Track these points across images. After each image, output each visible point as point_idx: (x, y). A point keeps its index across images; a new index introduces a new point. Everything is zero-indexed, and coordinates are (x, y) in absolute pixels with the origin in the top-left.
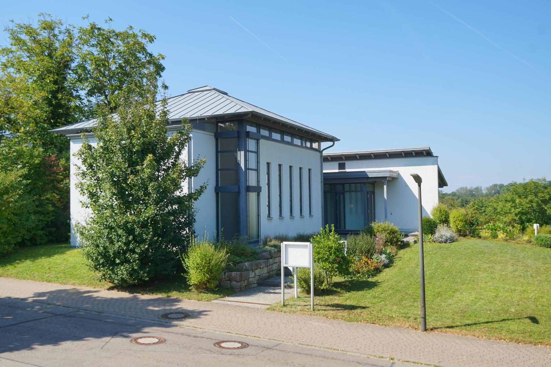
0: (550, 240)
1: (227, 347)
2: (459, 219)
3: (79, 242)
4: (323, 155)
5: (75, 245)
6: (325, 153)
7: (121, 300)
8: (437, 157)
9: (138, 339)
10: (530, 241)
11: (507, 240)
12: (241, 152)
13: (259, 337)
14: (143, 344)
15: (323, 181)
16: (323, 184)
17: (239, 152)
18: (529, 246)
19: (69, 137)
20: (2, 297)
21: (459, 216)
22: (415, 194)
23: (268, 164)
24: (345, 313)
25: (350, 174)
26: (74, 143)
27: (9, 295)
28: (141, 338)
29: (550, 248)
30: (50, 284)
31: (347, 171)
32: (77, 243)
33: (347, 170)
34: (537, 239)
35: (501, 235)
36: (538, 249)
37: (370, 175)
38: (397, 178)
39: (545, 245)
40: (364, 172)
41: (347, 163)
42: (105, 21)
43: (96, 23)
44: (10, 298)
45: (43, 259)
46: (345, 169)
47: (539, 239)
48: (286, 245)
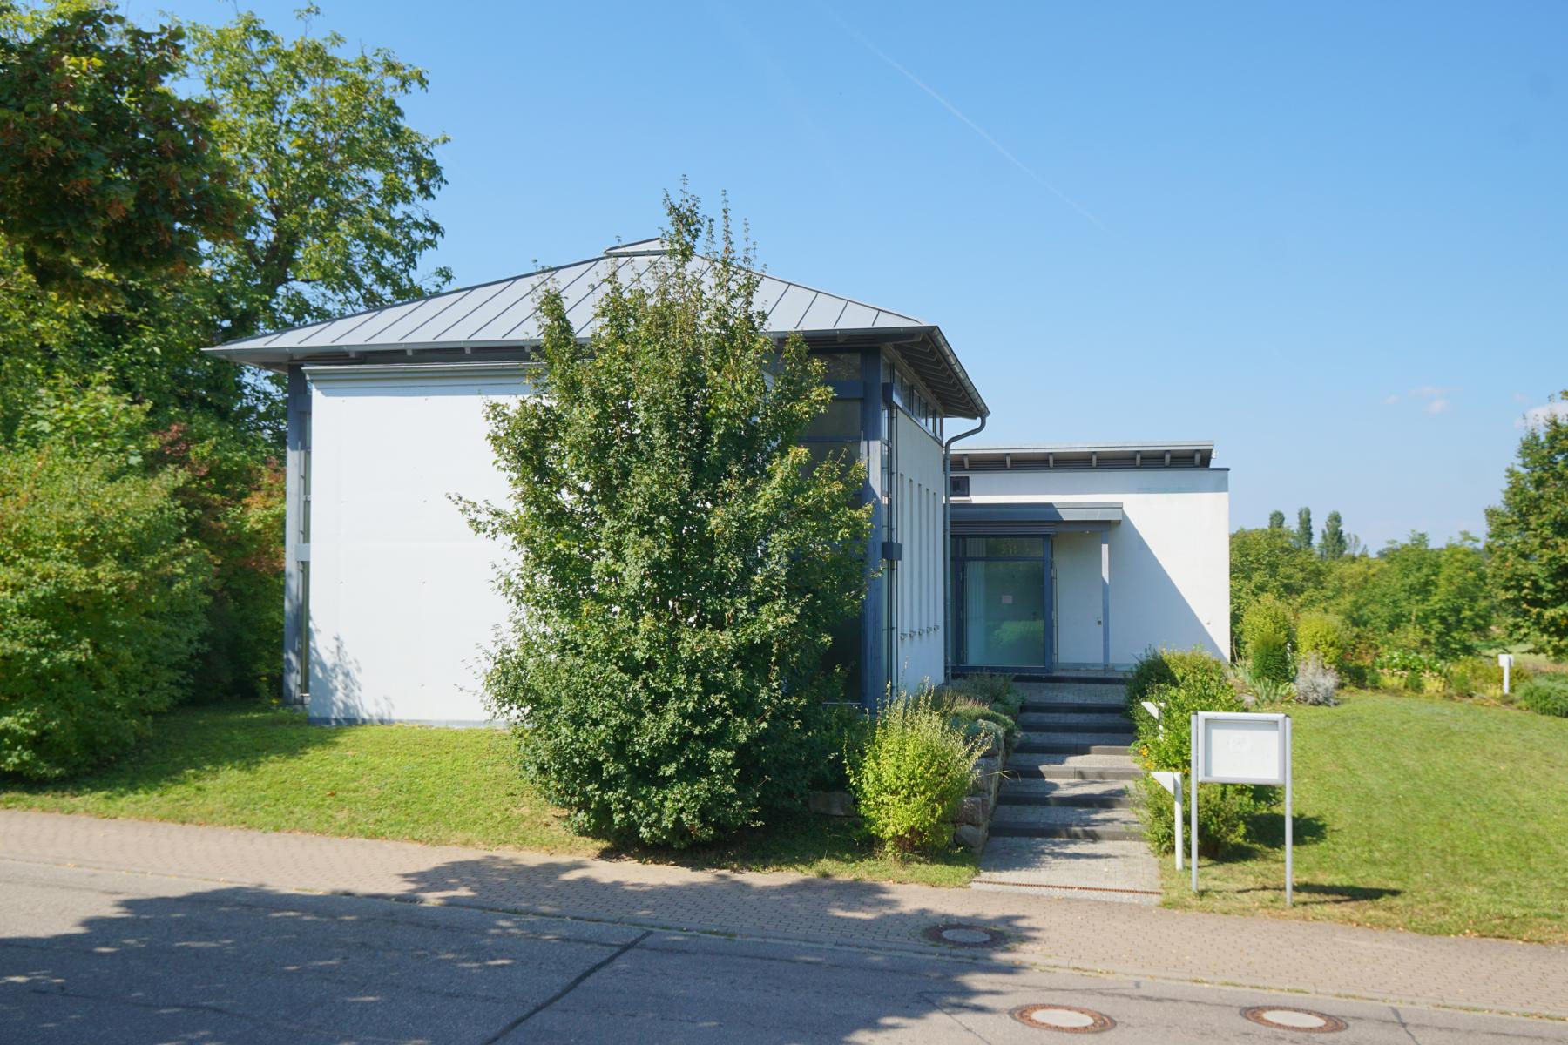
0: (1566, 697)
1: (1053, 1023)
2: (1328, 639)
3: (341, 705)
4: (951, 452)
5: (324, 716)
6: (957, 448)
7: (692, 887)
8: (1228, 469)
9: (1035, 1007)
10: (1509, 699)
11: (1451, 697)
12: (871, 443)
13: (1303, 992)
14: (1043, 1024)
15: (948, 528)
16: (948, 538)
17: (864, 444)
18: (1511, 712)
19: (310, 374)
20: (320, 893)
21: (1328, 633)
22: (1168, 573)
23: (911, 481)
24: (1348, 909)
25: (983, 510)
26: (326, 392)
27: (343, 886)
28: (1044, 1007)
29: (1566, 717)
30: (438, 849)
31: (974, 502)
32: (335, 709)
33: (975, 499)
34: (1532, 694)
35: (1432, 684)
36: (1528, 716)
37: (1067, 516)
38: (1119, 522)
39: (1556, 709)
40: (1050, 505)
41: (975, 479)
42: (297, 14)
43: (258, 17)
44: (348, 894)
45: (272, 762)
46: (968, 495)
47: (1535, 694)
48: (1207, 720)
